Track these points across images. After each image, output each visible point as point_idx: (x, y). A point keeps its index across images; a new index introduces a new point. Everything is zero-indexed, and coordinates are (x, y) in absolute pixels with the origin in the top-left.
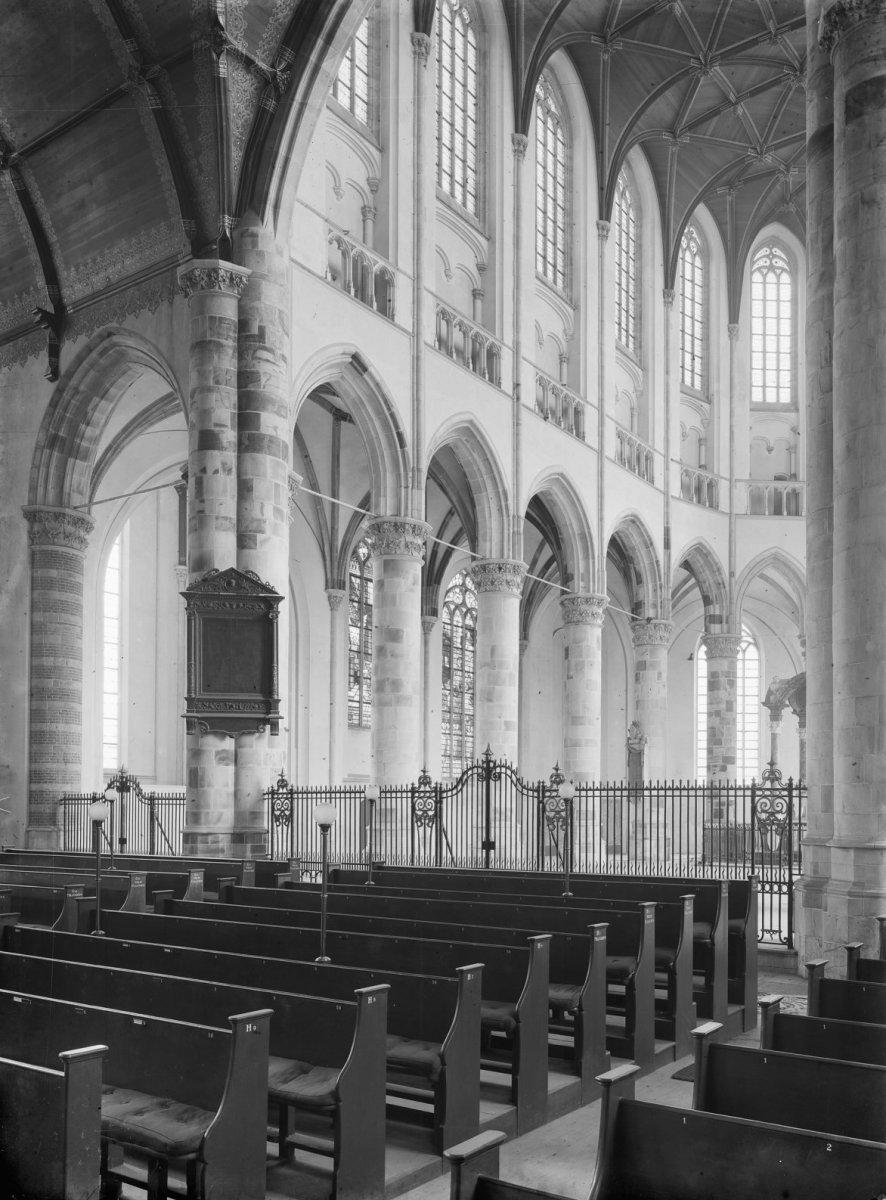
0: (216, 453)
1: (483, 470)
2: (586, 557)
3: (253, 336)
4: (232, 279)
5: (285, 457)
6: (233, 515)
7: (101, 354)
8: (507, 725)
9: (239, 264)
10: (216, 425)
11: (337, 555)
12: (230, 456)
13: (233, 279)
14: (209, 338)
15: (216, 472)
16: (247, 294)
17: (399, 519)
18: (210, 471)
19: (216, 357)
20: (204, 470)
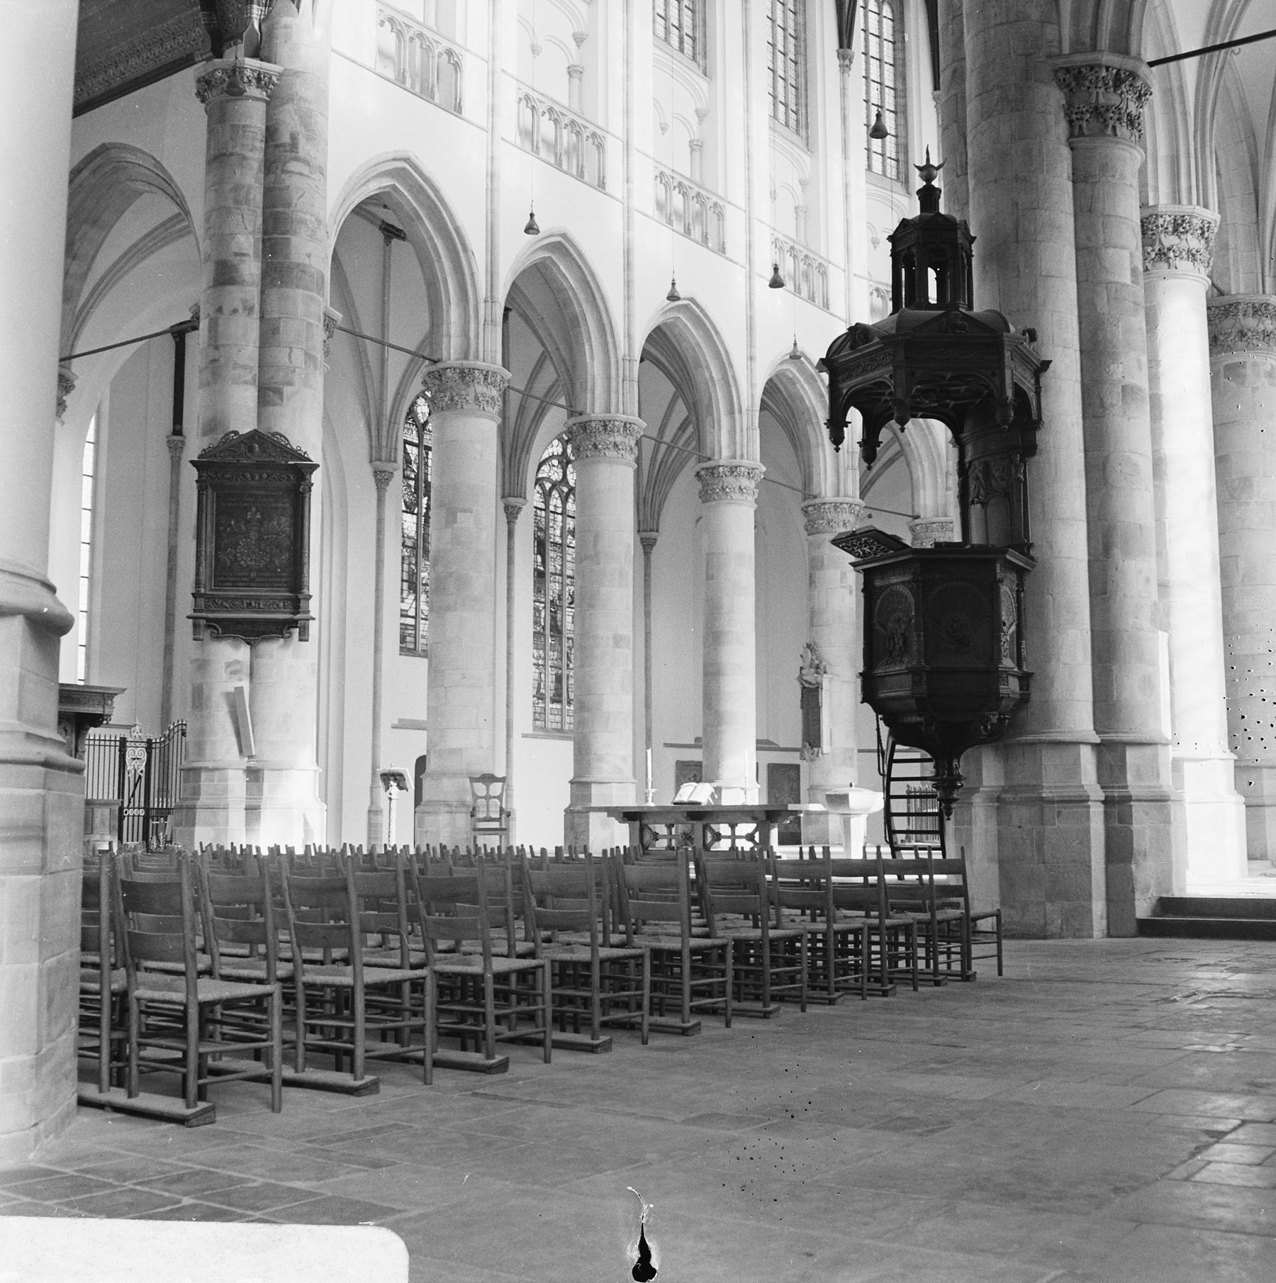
0: (233, 288)
1: (581, 296)
3: (283, 145)
4: (259, 79)
5: (320, 290)
6: (254, 364)
7: (94, 172)
9: (269, 61)
10: (236, 254)
11: (385, 422)
12: (252, 293)
13: (260, 80)
14: (230, 150)
15: (235, 311)
16: (275, 95)
17: (470, 363)
18: (226, 310)
19: (238, 172)
20: (220, 310)
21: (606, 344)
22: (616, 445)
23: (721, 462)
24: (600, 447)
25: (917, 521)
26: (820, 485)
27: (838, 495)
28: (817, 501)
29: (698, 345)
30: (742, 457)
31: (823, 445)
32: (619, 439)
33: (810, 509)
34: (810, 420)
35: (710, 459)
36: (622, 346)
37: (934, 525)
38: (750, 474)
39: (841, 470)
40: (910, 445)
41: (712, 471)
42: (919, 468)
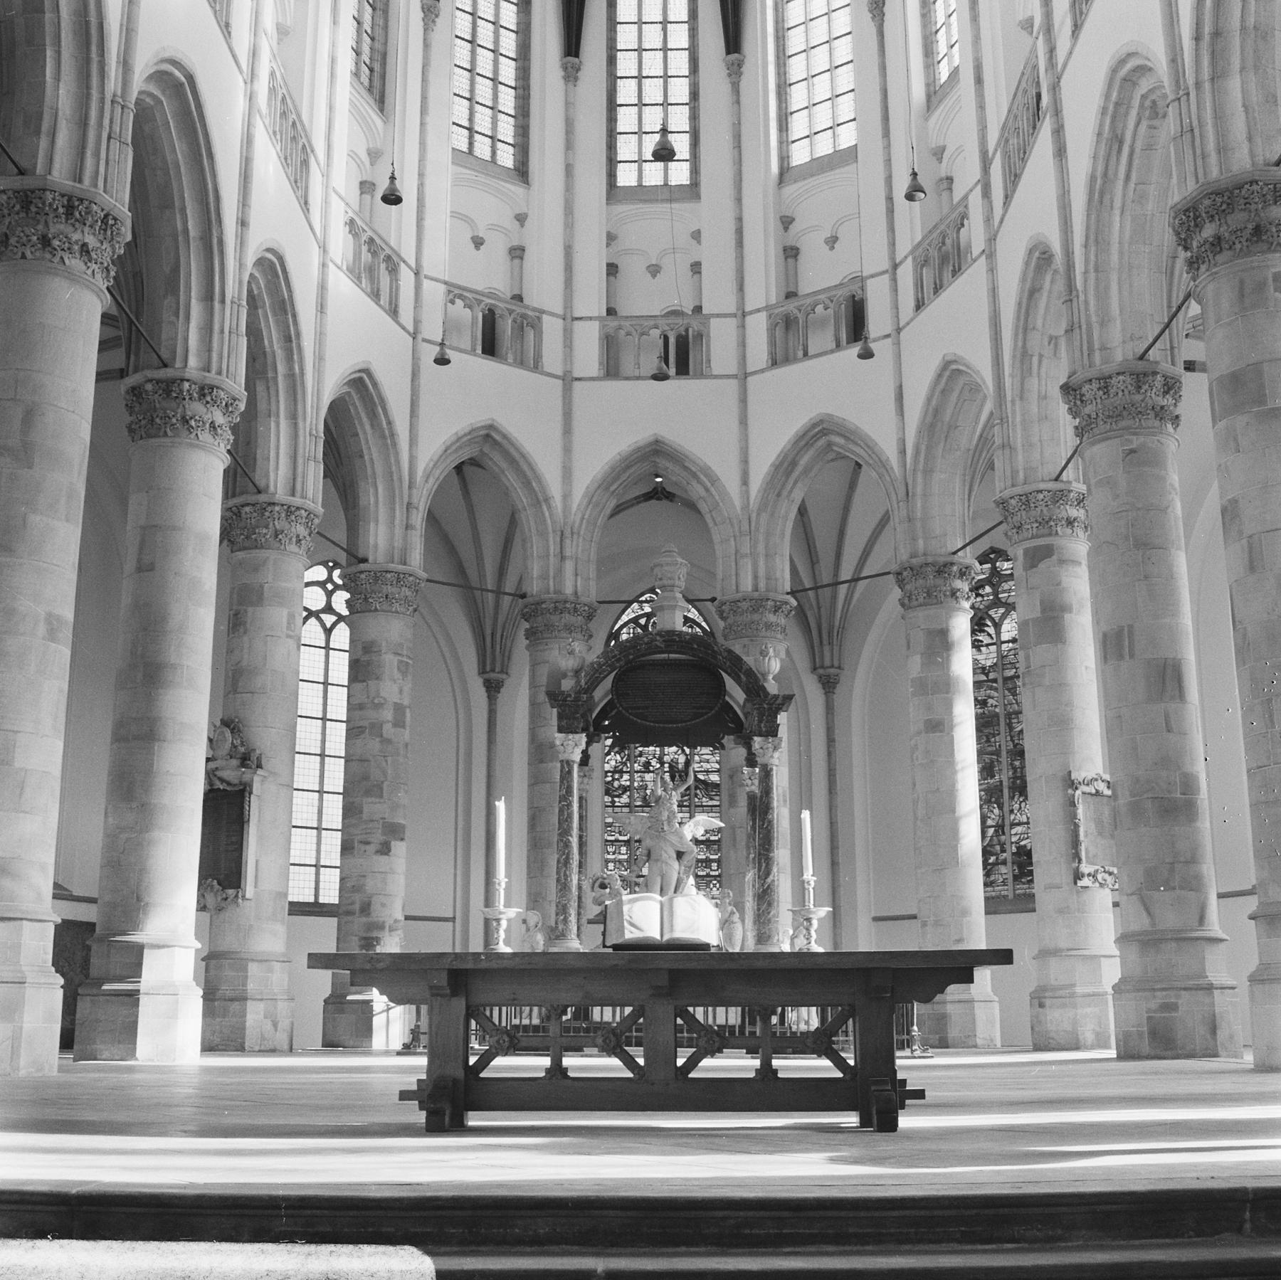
2: (208, 297)
8: (52, 622)
21: (87, 61)
22: (85, 250)
23: (187, 376)
24: (56, 243)
25: (362, 566)
26: (267, 476)
27: (293, 495)
28: (262, 498)
29: (178, 166)
30: (219, 373)
31: (278, 416)
32: (91, 241)
33: (247, 509)
34: (265, 372)
35: (165, 366)
36: (113, 74)
37: (389, 576)
38: (228, 408)
39: (300, 461)
40: (362, 456)
41: (170, 388)
42: (372, 491)
